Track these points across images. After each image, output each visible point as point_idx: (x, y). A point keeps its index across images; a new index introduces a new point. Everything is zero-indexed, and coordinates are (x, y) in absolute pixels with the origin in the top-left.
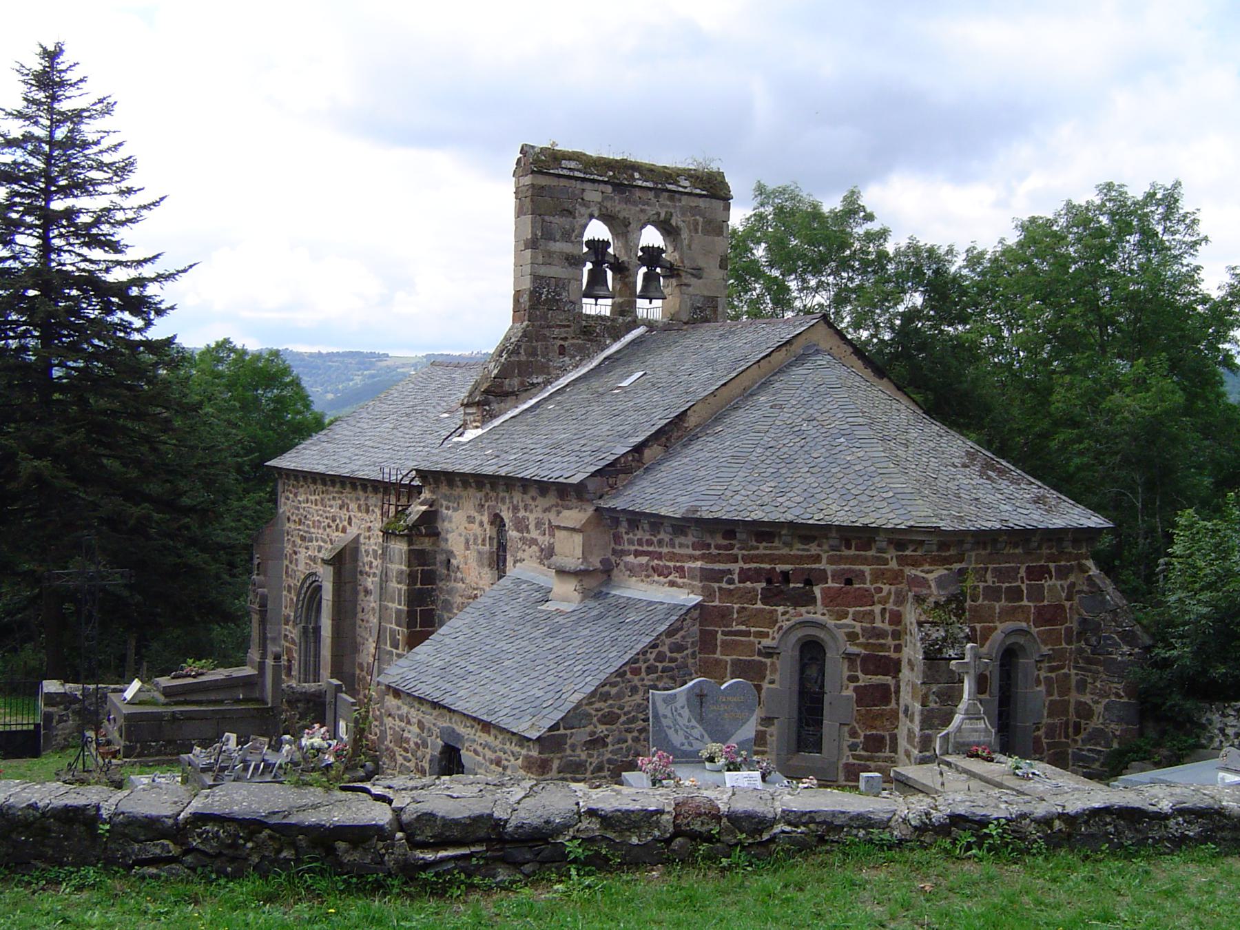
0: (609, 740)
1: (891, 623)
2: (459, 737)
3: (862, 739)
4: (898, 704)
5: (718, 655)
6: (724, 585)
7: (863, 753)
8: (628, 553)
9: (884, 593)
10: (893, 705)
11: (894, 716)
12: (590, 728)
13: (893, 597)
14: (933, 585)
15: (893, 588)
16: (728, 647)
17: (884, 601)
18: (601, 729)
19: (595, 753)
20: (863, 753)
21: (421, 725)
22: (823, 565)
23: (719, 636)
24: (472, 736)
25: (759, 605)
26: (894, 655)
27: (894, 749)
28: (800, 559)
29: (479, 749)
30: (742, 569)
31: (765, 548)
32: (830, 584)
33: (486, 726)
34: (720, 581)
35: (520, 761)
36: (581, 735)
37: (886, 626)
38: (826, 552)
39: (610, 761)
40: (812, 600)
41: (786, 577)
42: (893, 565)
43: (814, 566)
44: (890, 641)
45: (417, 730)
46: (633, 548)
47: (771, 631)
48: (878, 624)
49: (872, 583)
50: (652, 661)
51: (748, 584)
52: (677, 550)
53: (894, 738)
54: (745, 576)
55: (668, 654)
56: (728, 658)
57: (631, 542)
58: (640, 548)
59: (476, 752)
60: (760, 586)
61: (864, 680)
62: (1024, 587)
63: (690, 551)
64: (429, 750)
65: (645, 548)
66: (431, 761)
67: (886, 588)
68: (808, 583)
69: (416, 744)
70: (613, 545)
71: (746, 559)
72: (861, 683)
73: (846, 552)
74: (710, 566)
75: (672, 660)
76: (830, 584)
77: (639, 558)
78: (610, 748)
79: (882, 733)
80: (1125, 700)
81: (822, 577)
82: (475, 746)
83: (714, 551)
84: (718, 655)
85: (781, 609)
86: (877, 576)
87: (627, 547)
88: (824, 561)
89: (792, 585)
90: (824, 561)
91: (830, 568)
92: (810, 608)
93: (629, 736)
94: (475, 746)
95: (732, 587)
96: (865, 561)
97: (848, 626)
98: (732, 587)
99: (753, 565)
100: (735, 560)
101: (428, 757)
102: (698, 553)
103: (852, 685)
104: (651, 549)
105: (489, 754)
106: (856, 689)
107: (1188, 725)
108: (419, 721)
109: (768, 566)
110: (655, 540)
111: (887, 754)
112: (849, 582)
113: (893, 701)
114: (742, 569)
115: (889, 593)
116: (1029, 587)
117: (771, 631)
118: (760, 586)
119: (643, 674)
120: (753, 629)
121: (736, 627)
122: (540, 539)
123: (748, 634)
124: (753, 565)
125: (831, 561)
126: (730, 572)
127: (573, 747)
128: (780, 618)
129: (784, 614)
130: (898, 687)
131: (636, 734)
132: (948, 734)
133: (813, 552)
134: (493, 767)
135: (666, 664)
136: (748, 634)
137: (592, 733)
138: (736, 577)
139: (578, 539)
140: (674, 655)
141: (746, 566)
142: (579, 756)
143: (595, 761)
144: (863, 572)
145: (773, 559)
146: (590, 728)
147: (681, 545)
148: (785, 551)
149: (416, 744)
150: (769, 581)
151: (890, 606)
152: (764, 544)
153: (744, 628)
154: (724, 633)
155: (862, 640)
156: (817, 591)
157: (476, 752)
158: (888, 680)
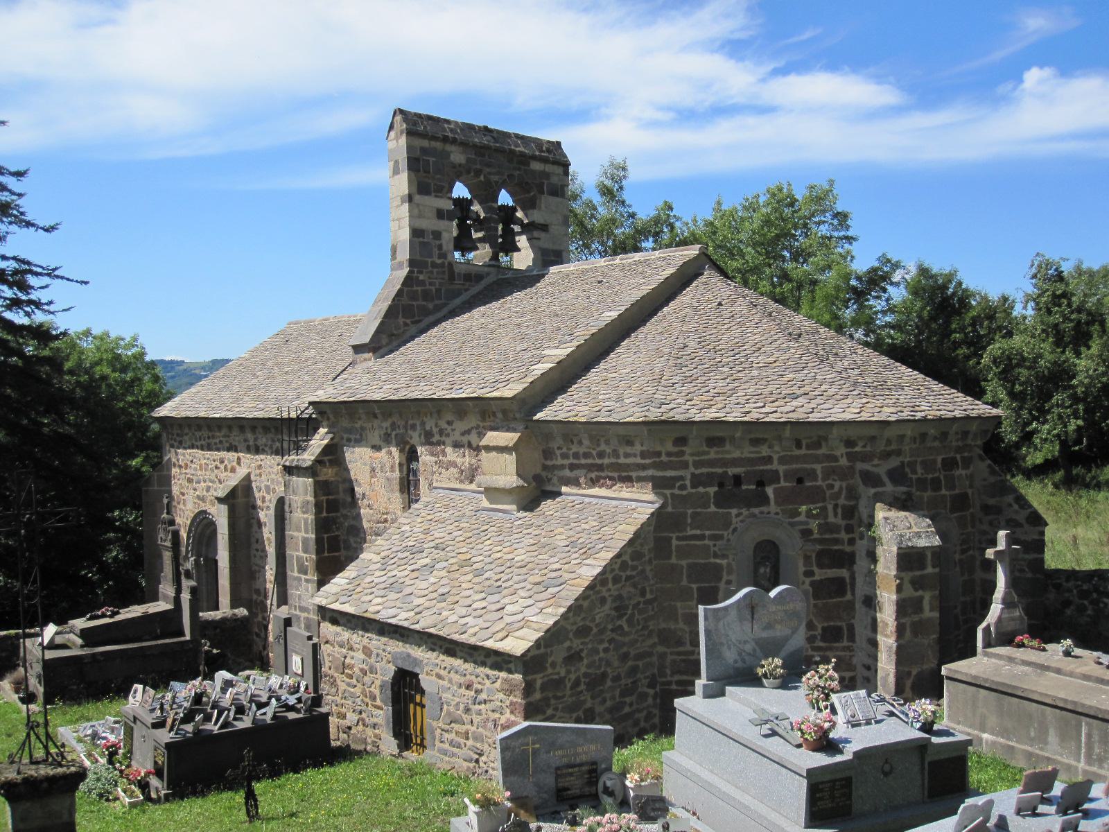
0: (583, 655)
1: (843, 518)
2: (416, 662)
3: (820, 631)
4: (853, 594)
5: (674, 560)
6: (676, 491)
7: (822, 644)
8: (562, 467)
9: (836, 489)
10: (849, 596)
11: (850, 606)
12: (567, 644)
13: (844, 492)
14: (886, 479)
15: (844, 484)
16: (682, 553)
17: (837, 496)
18: (577, 644)
19: (573, 669)
20: (822, 644)
21: (367, 652)
22: (775, 466)
23: (674, 542)
24: (433, 661)
25: (713, 508)
26: (848, 549)
27: (852, 638)
28: (751, 462)
29: (442, 672)
30: (693, 475)
31: (717, 452)
32: (783, 484)
33: (450, 647)
34: (672, 487)
35: (498, 685)
36: (559, 653)
37: (842, 523)
38: (778, 453)
39: (586, 675)
40: (764, 500)
41: (737, 480)
42: (844, 462)
43: (765, 468)
44: (844, 536)
45: (362, 656)
46: (566, 462)
47: (725, 533)
48: (831, 519)
49: (824, 479)
50: (617, 572)
51: (701, 489)
52: (622, 460)
53: (851, 629)
54: (697, 481)
55: (630, 563)
56: (684, 563)
57: (565, 456)
58: (575, 462)
59: (439, 676)
60: (712, 490)
61: (820, 574)
62: (942, 477)
63: (639, 460)
64: (378, 676)
65: (583, 461)
66: (382, 687)
67: (837, 485)
68: (761, 484)
69: (362, 670)
70: (543, 461)
71: (697, 464)
72: (817, 578)
73: (797, 452)
74: (660, 474)
75: (634, 568)
76: (783, 484)
77: (575, 472)
78: (585, 661)
79: (839, 624)
80: (1029, 575)
81: (774, 477)
82: (437, 670)
83: (664, 458)
84: (674, 560)
85: (734, 511)
86: (828, 474)
87: (560, 462)
88: (775, 462)
89: (744, 487)
90: (775, 462)
91: (782, 469)
92: (762, 509)
93: (601, 647)
94: (437, 670)
95: (684, 493)
96: (817, 459)
97: (801, 523)
98: (684, 493)
99: (704, 470)
100: (685, 465)
101: (378, 683)
102: (647, 461)
103: (808, 581)
104: (589, 461)
105: (456, 678)
106: (812, 584)
107: (1095, 595)
108: (364, 647)
109: (719, 470)
110: (594, 453)
111: (845, 643)
112: (800, 481)
113: (849, 592)
114: (693, 475)
115: (841, 488)
116: (945, 476)
117: (725, 533)
118: (712, 490)
119: (610, 585)
120: (707, 533)
121: (690, 532)
122: (459, 461)
123: (702, 537)
124: (704, 470)
125: (782, 460)
126: (682, 478)
127: (553, 665)
128: (734, 520)
129: (738, 515)
130: (853, 578)
131: (606, 645)
132: (988, 626)
133: (764, 454)
134: (463, 690)
135: (629, 573)
136: (702, 537)
137: (570, 648)
138: (688, 483)
139: (510, 460)
140: (635, 563)
141: (697, 472)
142: (558, 673)
143: (573, 677)
144: (814, 471)
145: (725, 463)
146: (567, 644)
147: (627, 455)
148: (737, 454)
149: (362, 670)
150: (721, 485)
151: (842, 501)
152: (715, 449)
153: (698, 532)
154: (678, 538)
155: (816, 536)
156: (770, 491)
157: (439, 676)
158: (844, 573)
